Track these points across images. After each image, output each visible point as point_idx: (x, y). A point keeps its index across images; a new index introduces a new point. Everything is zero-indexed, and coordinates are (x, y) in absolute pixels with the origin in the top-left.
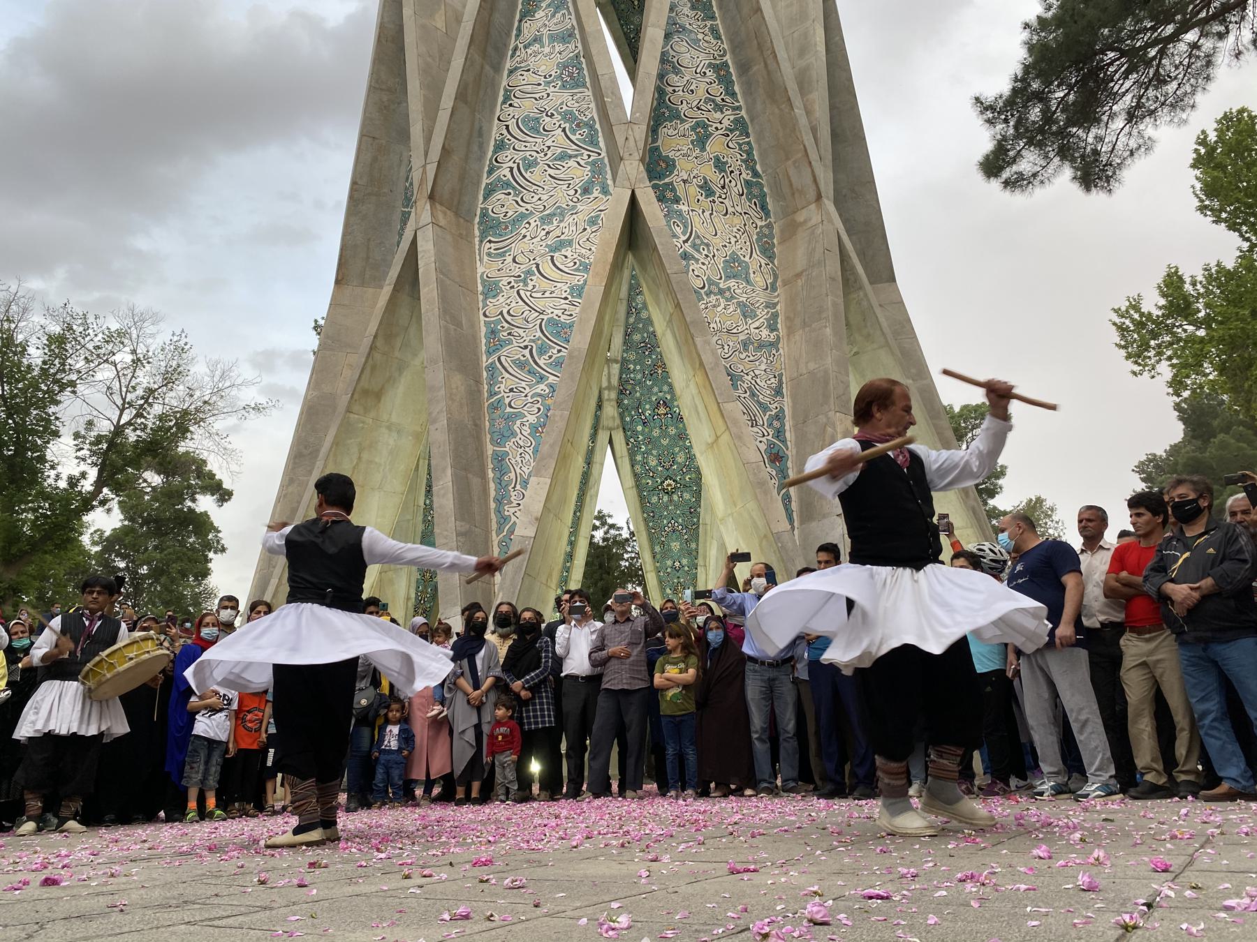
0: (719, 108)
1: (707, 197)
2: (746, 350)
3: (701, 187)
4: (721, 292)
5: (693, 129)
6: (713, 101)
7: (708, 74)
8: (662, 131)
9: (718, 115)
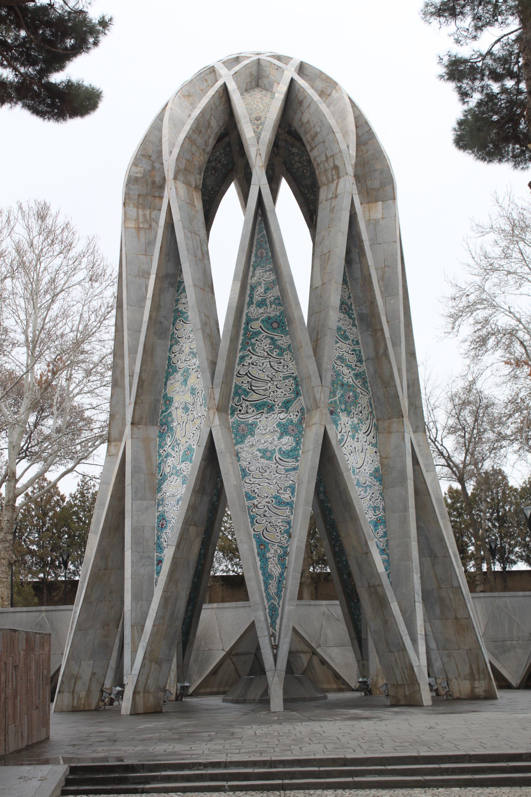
0: (194, 355)
1: (186, 412)
2: (178, 504)
3: (183, 409)
4: (177, 472)
5: (182, 374)
6: (192, 353)
7: (191, 336)
8: (169, 382)
9: (194, 360)
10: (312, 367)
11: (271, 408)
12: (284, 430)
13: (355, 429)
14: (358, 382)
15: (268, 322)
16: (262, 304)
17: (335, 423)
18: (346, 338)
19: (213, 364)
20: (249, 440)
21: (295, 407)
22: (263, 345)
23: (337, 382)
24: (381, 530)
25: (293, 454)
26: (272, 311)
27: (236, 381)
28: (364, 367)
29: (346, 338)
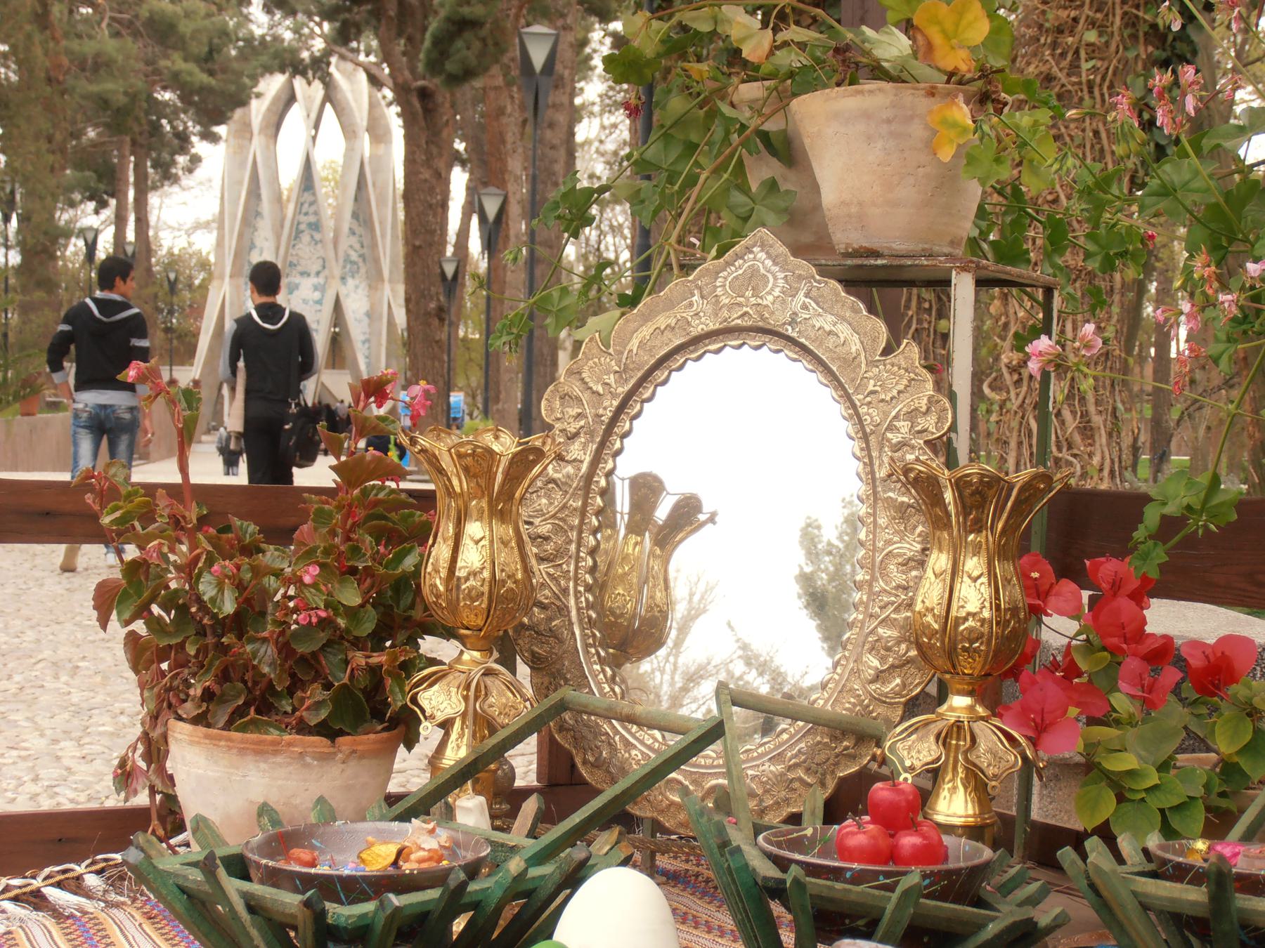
10: (331, 254)
11: (309, 275)
12: (316, 288)
13: (357, 287)
14: (361, 260)
15: (310, 225)
16: (306, 214)
17: (345, 284)
18: (354, 233)
19: (278, 248)
20: (296, 293)
21: (322, 275)
22: (306, 238)
23: (347, 260)
24: (367, 345)
25: (319, 302)
26: (312, 219)
27: (290, 258)
28: (365, 251)
29: (354, 233)
